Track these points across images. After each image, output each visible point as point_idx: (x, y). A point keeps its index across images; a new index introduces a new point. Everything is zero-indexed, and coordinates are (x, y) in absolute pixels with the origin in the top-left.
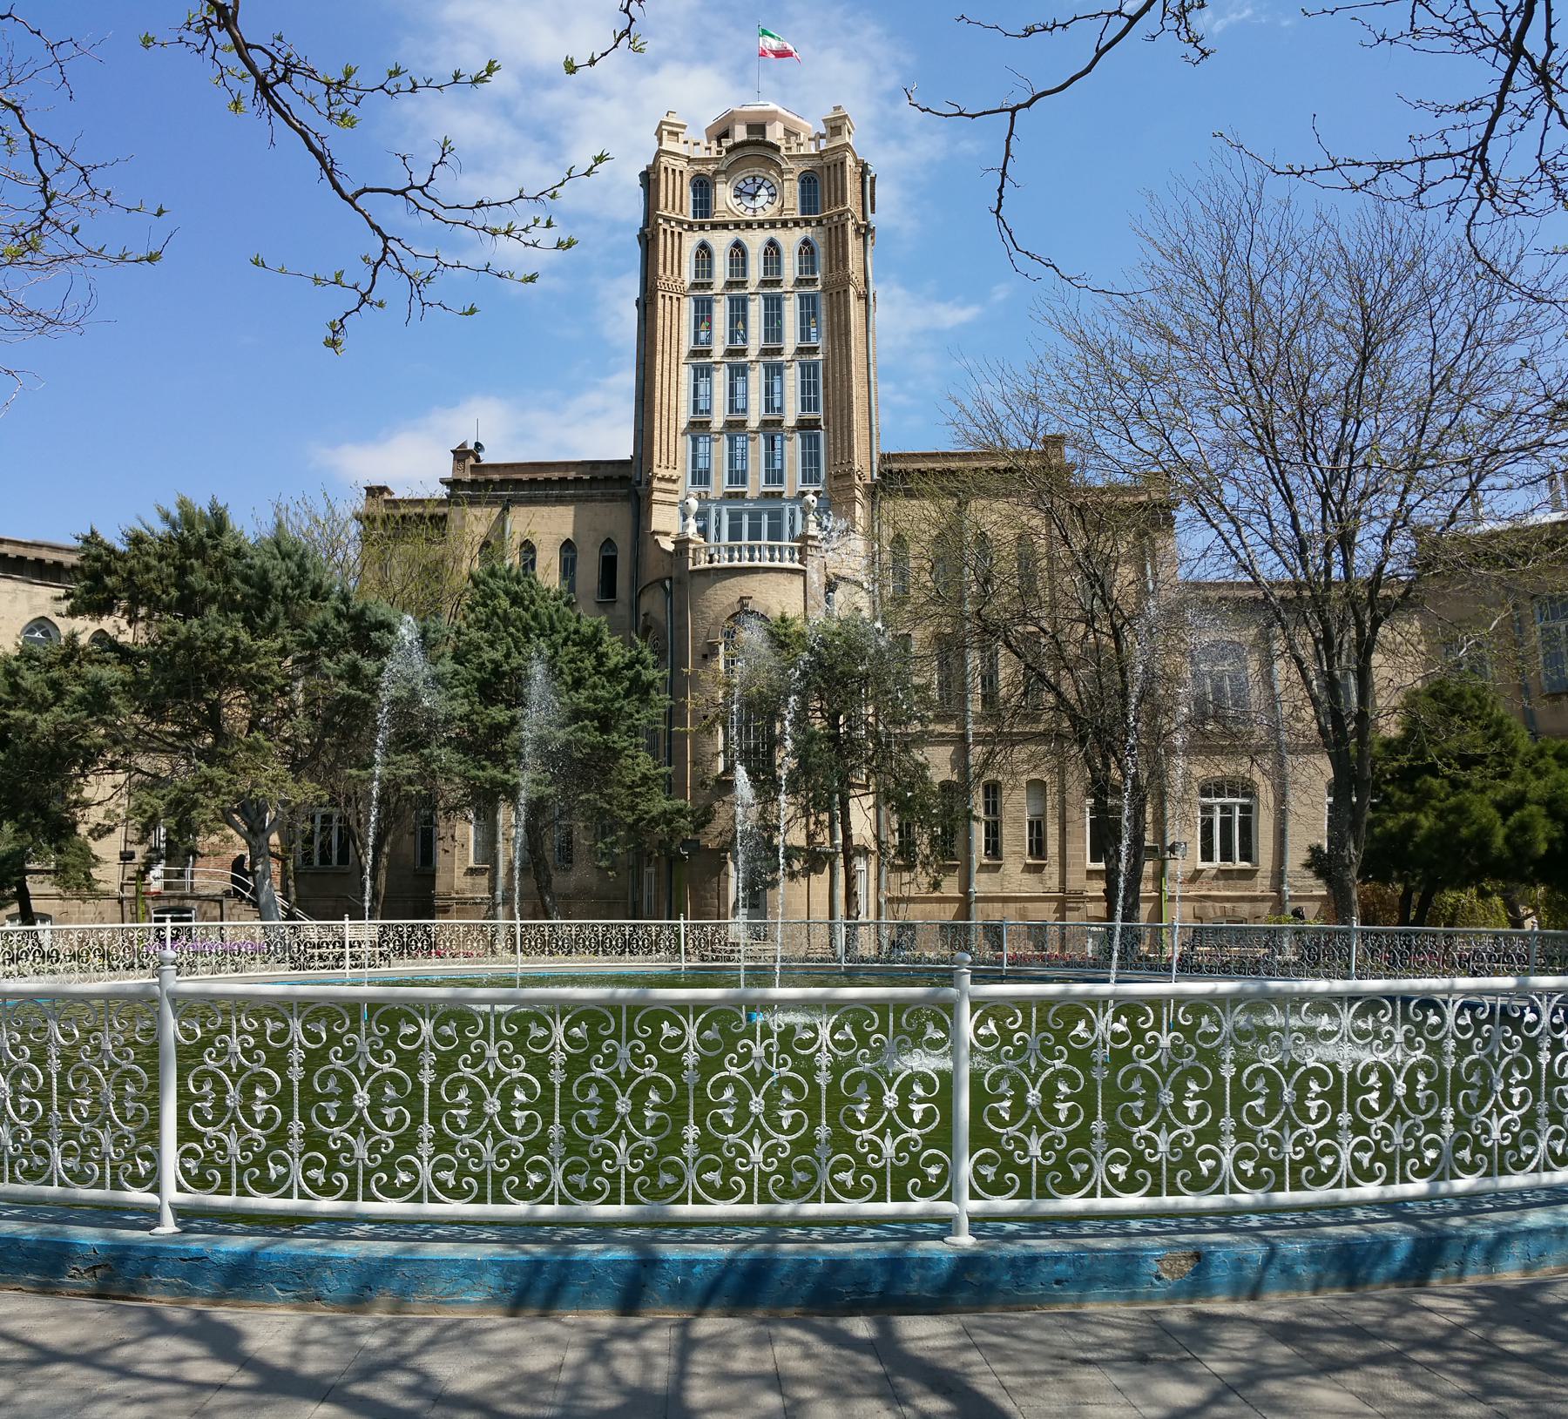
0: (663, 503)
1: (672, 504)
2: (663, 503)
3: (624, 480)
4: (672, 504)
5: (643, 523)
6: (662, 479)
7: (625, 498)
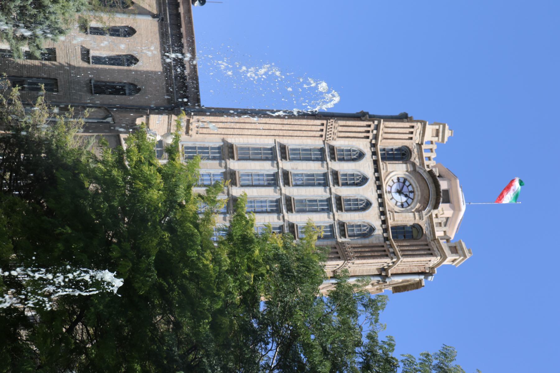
0: (169, 124)
6: (188, 121)
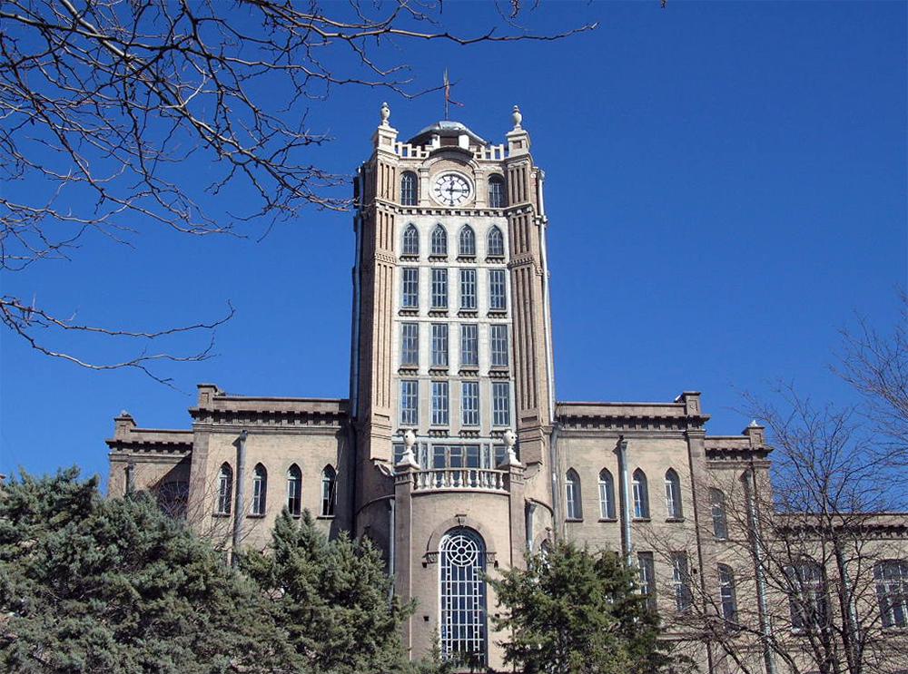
0: (380, 436)
1: (387, 438)
2: (380, 436)
4: (387, 438)
5: (359, 453)
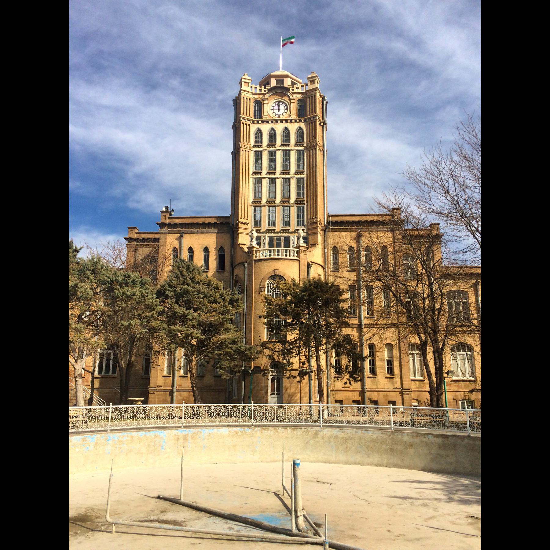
0: (243, 233)
1: (247, 234)
2: (243, 233)
3: (227, 224)
4: (247, 234)
5: (235, 241)
6: (242, 223)
7: (228, 232)
